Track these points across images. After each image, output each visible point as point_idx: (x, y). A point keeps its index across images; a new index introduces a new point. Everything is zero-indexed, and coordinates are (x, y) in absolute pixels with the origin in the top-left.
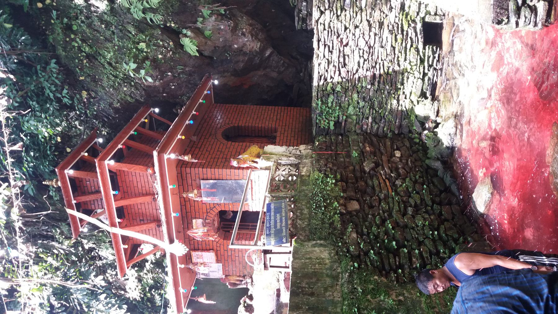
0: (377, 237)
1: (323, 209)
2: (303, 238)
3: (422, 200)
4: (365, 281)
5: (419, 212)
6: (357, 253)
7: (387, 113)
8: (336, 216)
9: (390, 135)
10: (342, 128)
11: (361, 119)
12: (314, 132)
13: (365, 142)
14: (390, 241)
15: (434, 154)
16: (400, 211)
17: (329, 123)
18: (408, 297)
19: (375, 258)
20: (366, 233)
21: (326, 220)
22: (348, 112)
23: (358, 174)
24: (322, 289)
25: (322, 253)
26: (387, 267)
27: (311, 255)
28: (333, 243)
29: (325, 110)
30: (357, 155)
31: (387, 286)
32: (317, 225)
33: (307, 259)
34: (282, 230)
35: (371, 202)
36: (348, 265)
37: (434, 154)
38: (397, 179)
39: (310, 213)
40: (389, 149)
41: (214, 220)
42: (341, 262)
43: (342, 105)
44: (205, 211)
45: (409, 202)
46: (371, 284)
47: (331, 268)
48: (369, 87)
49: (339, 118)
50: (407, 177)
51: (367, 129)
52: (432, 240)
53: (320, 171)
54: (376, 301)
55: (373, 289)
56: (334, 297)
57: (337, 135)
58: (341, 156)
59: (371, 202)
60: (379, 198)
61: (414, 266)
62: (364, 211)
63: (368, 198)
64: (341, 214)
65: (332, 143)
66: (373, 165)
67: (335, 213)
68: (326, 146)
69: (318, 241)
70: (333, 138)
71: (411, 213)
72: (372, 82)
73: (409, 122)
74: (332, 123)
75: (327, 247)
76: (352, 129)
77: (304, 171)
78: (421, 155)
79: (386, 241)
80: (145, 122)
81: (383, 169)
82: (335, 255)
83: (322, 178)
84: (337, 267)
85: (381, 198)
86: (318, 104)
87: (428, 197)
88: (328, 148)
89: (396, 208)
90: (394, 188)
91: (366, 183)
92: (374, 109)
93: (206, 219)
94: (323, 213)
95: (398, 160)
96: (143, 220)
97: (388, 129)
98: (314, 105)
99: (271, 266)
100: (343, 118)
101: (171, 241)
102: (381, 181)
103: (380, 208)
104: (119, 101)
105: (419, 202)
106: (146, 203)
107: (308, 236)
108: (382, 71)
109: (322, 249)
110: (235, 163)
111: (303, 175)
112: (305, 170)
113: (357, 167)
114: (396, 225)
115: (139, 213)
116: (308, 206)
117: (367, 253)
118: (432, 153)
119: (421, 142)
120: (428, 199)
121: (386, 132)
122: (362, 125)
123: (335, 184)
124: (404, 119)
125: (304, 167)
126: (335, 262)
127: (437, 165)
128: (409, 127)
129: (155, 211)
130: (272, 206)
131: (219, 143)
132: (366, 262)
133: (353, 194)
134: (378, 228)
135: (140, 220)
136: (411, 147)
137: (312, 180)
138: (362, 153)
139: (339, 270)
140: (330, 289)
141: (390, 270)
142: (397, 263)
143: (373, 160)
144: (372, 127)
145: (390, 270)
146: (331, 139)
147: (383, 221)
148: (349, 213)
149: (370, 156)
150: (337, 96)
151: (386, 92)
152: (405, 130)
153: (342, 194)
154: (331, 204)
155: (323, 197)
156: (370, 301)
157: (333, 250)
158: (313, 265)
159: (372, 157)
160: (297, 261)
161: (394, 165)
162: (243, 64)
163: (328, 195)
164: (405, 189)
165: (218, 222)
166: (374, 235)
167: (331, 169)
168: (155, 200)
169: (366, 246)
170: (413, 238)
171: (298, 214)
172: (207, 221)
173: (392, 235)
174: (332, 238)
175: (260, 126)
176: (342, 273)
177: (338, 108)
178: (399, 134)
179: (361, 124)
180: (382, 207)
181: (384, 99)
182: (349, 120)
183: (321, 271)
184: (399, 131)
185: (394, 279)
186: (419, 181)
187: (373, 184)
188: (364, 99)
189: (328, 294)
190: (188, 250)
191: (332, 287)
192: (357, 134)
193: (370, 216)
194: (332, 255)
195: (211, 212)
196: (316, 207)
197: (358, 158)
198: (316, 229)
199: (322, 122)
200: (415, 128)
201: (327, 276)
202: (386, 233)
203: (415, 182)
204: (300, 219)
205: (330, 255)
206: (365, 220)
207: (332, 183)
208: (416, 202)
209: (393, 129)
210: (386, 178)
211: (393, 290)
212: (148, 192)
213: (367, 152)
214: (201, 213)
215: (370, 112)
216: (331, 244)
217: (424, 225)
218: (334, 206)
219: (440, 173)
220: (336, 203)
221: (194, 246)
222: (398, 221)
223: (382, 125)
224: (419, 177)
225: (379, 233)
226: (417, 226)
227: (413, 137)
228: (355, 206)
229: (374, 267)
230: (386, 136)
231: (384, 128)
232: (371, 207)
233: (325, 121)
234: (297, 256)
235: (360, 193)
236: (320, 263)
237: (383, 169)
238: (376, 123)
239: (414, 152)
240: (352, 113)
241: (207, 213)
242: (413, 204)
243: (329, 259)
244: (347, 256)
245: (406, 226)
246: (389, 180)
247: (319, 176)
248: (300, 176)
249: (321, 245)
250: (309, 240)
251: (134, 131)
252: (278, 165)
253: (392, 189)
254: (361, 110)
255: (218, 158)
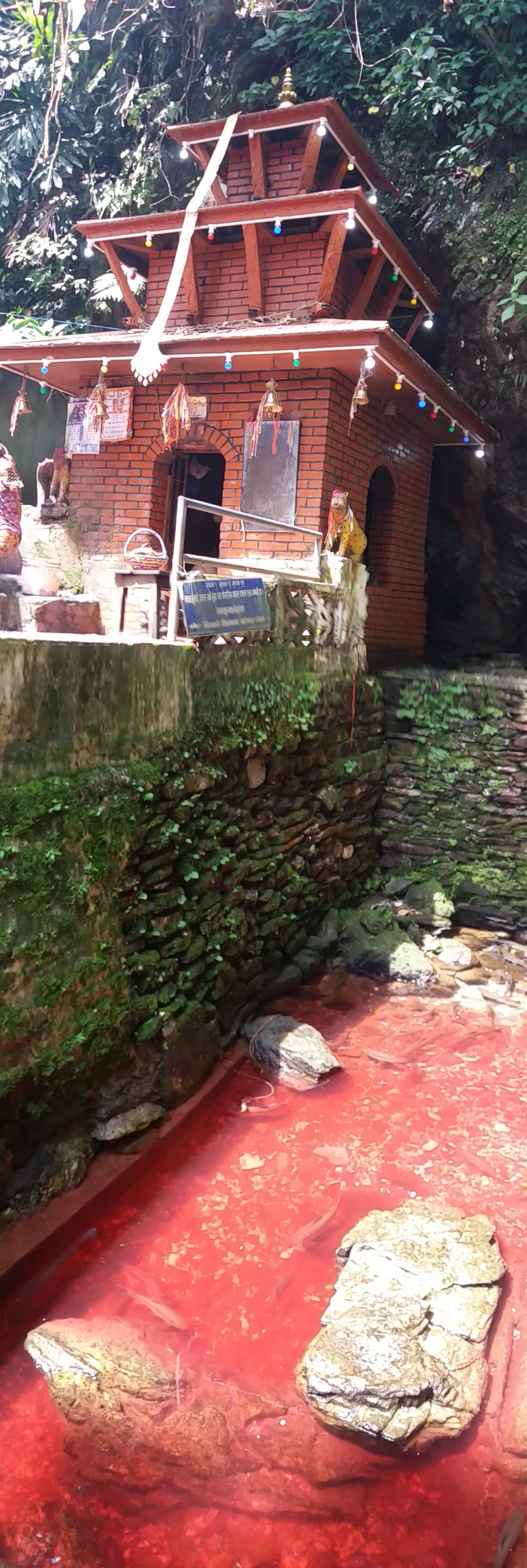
0: (201, 834)
1: (254, 709)
2: (197, 666)
3: (269, 915)
4: (119, 820)
5: (250, 913)
6: (170, 794)
7: (425, 827)
8: (240, 739)
9: (378, 831)
10: (399, 735)
11: (416, 774)
12: (390, 674)
13: (369, 784)
14: (196, 865)
15: (348, 923)
16: (251, 874)
17: (411, 707)
18: (94, 922)
19: (164, 839)
20: (208, 808)
21: (233, 717)
22: (433, 749)
23: (312, 777)
24: (95, 722)
25: (167, 717)
26: (148, 865)
27: (163, 689)
28: (188, 738)
29: (443, 701)
30: (350, 770)
31: (111, 874)
32: (223, 698)
33: (157, 679)
34: (214, 621)
35: (263, 809)
36: (146, 778)
37: (348, 923)
38: (305, 858)
39: (245, 679)
40: (355, 834)
41: (198, 442)
42: (150, 759)
43: (451, 736)
44: (226, 425)
45: (266, 889)
46: (113, 838)
47: (138, 738)
48: (487, 793)
49: (421, 727)
50: (308, 877)
51: (394, 785)
52: (204, 952)
53: (321, 694)
54: (79, 853)
55: (104, 843)
56: (77, 752)
57: (383, 724)
58: (346, 735)
59: (263, 809)
60: (269, 827)
61: (153, 922)
62: (248, 797)
63: (271, 803)
64: (241, 751)
65: (369, 713)
66: (331, 807)
67: (245, 737)
68: (364, 703)
69: (191, 703)
70: (378, 715)
71: (247, 898)
72: (497, 799)
73: (405, 868)
74: (410, 714)
75: (180, 725)
76: (394, 754)
77: (320, 658)
78: (346, 896)
79: (196, 856)
80: (411, 298)
81: (322, 828)
82: (163, 743)
83: (309, 701)
84: (139, 752)
85: (271, 831)
86: (455, 685)
87: (276, 924)
88: (362, 707)
89: (256, 865)
90: (289, 855)
91: (297, 794)
92: (436, 801)
93: (206, 426)
94: (244, 709)
95: (338, 855)
96: (204, 284)
97: (390, 828)
98: (454, 677)
99: (126, 591)
100: (421, 735)
101: (165, 348)
102: (300, 827)
103: (254, 832)
104: (457, 244)
105: (266, 909)
106: (243, 294)
107: (201, 679)
108: (514, 820)
109: (177, 713)
110: (338, 499)
111: (313, 656)
112: (323, 659)
113: (325, 773)
114: (227, 871)
115: (221, 276)
116: (258, 673)
117: (171, 815)
118: (352, 920)
119: (364, 892)
120: (270, 926)
121: (384, 823)
122: (402, 777)
123: (299, 732)
124: (413, 860)
125: (327, 656)
126: (151, 746)
127: (329, 933)
128: (396, 867)
129: (226, 311)
130: (256, 592)
131: (369, 460)
132: (155, 815)
133: (278, 769)
134: (218, 834)
135: (204, 278)
136: (358, 876)
137: (304, 678)
138: (350, 781)
139: (133, 758)
140: (95, 740)
141: (142, 874)
142: (156, 887)
143: (338, 805)
144: (397, 795)
145: (142, 874)
146: (376, 711)
147: (229, 843)
148: (243, 767)
149: (344, 798)
150: (471, 727)
151: (471, 827)
152: (388, 861)
153: (279, 747)
154: (262, 726)
155: (276, 706)
156: (78, 840)
157: (175, 739)
158: (145, 694)
159: (344, 802)
160: (153, 656)
161: (329, 848)
162: (515, 512)
163: (279, 718)
164: (290, 878)
165: (194, 449)
166: (206, 827)
167: (323, 718)
168: (253, 314)
169: (186, 813)
170: (205, 910)
171: (243, 651)
172: (201, 428)
173: (208, 865)
174: (199, 735)
175: (392, 548)
176: (128, 765)
177: (446, 727)
178: (380, 850)
179: (405, 774)
180: (255, 836)
181: (455, 823)
182: (415, 750)
183: (132, 715)
184: (386, 848)
185: (128, 885)
186: (302, 901)
187: (295, 810)
188: (461, 781)
189: (85, 736)
190: (145, 383)
191: (100, 744)
192: (383, 767)
193: (239, 811)
194: (164, 739)
195: (223, 439)
196: (256, 693)
197: (342, 773)
198: (216, 694)
199: (415, 693)
200: (393, 879)
201: (123, 732)
202: (211, 854)
203: (301, 896)
204: (232, 656)
205: (164, 733)
206: (233, 802)
207: (300, 723)
208: (264, 903)
209: (390, 836)
210: (306, 836)
211: (105, 887)
212: (269, 300)
213: (353, 790)
214: (221, 416)
215: (430, 792)
216: (186, 733)
217: (227, 929)
218: (260, 733)
219: (314, 941)
220: (265, 737)
221: (147, 399)
222: (234, 874)
223: (400, 816)
224: (309, 902)
225: (210, 837)
226: (225, 916)
227: (374, 876)
228: (256, 777)
229: (146, 838)
230: (375, 823)
231: (394, 819)
232: (255, 811)
233: (415, 699)
234: (162, 657)
235: (279, 784)
236: (147, 710)
237: (322, 828)
238: (405, 805)
239: (349, 883)
240: (431, 757)
241: (220, 430)
242: (263, 898)
243: (156, 731)
244: (162, 773)
245: (224, 892)
246: (303, 841)
247: (311, 693)
248: (311, 650)
249: (184, 710)
250: (194, 681)
251: (399, 276)
252: (331, 599)
253: (287, 851)
254: (435, 776)
255: (342, 461)
